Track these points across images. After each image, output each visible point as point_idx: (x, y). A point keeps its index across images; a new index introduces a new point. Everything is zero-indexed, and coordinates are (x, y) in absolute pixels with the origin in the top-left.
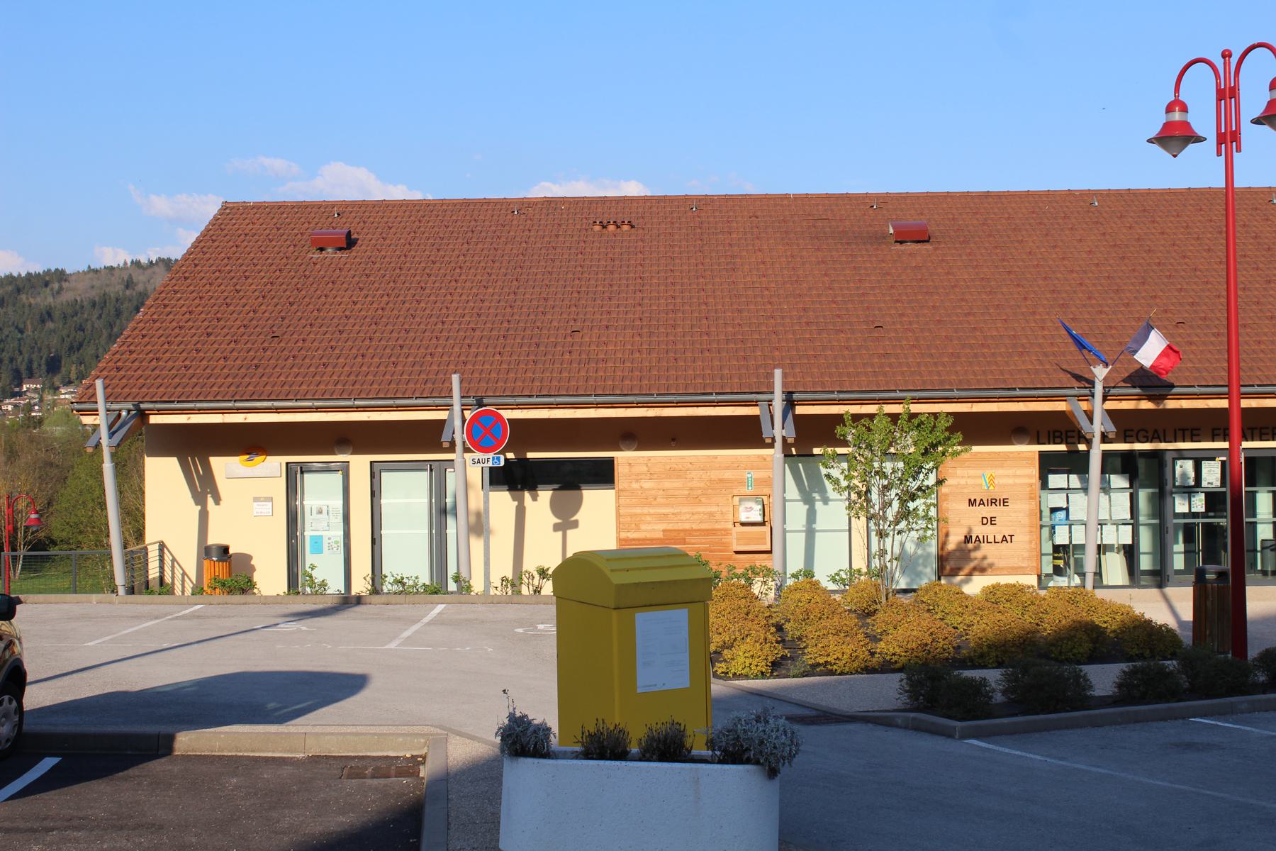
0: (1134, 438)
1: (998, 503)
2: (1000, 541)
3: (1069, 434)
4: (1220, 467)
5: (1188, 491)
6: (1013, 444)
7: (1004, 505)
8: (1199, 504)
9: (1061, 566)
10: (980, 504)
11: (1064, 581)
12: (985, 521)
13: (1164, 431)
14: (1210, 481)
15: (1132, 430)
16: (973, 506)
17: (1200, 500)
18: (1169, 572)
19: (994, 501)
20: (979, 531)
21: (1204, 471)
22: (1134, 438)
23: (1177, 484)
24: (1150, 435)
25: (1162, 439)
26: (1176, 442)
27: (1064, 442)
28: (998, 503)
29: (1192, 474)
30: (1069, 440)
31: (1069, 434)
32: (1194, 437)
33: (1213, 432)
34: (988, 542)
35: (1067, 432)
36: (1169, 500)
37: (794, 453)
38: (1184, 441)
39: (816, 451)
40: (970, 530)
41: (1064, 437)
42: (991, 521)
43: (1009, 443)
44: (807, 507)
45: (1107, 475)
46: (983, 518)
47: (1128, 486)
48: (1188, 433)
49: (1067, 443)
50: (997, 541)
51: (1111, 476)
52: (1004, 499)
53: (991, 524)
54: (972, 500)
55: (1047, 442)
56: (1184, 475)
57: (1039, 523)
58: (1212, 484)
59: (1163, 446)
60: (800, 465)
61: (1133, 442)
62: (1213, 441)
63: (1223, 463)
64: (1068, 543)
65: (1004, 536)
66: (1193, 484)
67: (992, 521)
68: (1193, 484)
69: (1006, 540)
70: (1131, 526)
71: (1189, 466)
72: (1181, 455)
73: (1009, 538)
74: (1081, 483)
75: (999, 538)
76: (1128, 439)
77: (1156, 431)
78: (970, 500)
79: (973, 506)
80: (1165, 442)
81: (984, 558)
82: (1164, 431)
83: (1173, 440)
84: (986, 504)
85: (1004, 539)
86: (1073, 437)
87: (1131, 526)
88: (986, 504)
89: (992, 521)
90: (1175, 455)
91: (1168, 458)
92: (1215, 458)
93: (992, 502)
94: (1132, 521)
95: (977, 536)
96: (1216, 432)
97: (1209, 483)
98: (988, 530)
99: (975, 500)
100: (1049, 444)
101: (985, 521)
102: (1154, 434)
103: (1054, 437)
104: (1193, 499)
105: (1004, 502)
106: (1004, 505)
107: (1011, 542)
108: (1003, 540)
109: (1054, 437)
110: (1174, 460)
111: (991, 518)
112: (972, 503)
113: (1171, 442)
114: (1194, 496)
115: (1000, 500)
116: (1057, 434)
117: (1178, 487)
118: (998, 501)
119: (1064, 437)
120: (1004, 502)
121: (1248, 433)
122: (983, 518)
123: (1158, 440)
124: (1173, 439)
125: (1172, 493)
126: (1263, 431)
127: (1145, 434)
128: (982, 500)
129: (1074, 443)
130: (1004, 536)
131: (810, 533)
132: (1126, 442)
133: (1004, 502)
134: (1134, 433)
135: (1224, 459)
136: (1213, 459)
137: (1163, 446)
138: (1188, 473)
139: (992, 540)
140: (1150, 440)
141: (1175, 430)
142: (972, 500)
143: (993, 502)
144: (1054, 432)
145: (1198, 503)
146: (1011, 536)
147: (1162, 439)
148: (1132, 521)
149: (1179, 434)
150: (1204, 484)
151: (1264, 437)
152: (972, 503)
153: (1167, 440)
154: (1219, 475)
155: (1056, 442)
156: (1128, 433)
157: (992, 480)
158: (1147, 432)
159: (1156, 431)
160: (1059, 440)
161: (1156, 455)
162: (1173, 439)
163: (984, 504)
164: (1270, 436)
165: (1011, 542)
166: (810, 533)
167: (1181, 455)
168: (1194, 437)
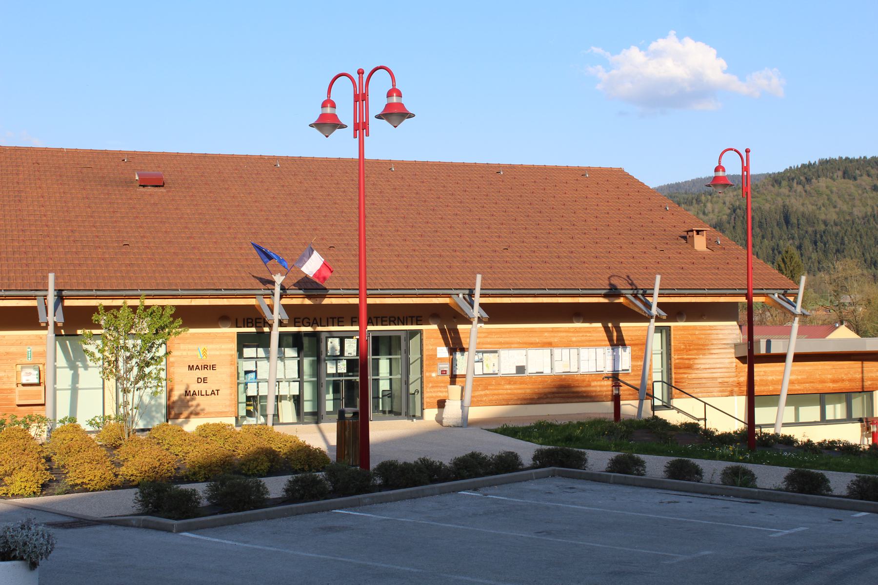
0: (301, 324)
1: (208, 368)
5: (336, 359)
6: (220, 328)
8: (342, 367)
9: (252, 410)
10: (196, 369)
13: (321, 319)
15: (300, 318)
16: (191, 370)
17: (343, 365)
18: (323, 413)
20: (194, 387)
22: (301, 324)
23: (329, 354)
24: (311, 322)
25: (319, 325)
26: (328, 326)
27: (254, 325)
28: (208, 368)
29: (338, 348)
30: (258, 325)
31: (258, 321)
32: (340, 323)
34: (201, 395)
36: (323, 365)
37: (63, 333)
38: (333, 326)
39: (79, 332)
40: (188, 386)
41: (254, 322)
42: (204, 380)
43: (218, 327)
44: (72, 372)
45: (283, 348)
46: (198, 378)
47: (297, 356)
49: (256, 327)
51: (286, 349)
54: (191, 366)
55: (242, 326)
56: (333, 348)
58: (351, 354)
59: (319, 329)
60: (68, 342)
61: (300, 326)
63: (358, 339)
64: (256, 395)
66: (339, 354)
67: (205, 380)
68: (339, 354)
69: (214, 394)
70: (298, 383)
72: (331, 335)
73: (216, 392)
75: (209, 392)
77: (315, 319)
78: (189, 366)
79: (191, 370)
81: (198, 405)
82: (321, 319)
84: (200, 368)
85: (213, 393)
87: (298, 383)
88: (200, 369)
89: (205, 380)
90: (327, 335)
91: (323, 336)
92: (353, 337)
93: (204, 368)
94: (299, 379)
95: (194, 391)
97: (349, 353)
98: (202, 387)
99: (193, 366)
100: (244, 327)
102: (314, 321)
103: (248, 323)
104: (338, 364)
105: (213, 367)
107: (218, 394)
108: (212, 394)
110: (327, 338)
111: (204, 378)
112: (191, 368)
113: (325, 326)
114: (339, 362)
117: (329, 356)
118: (209, 367)
119: (254, 322)
120: (213, 367)
121: (374, 321)
122: (198, 378)
125: (325, 360)
126: (384, 319)
127: (308, 320)
128: (197, 366)
129: (261, 327)
130: (213, 391)
131: (74, 391)
132: (295, 326)
133: (213, 367)
134: (301, 320)
135: (358, 337)
136: (352, 337)
137: (319, 329)
138: (336, 347)
142: (191, 366)
143: (205, 367)
144: (247, 319)
146: (218, 390)
147: (319, 325)
148: (299, 379)
149: (330, 320)
150: (346, 354)
152: (191, 368)
153: (322, 325)
156: (297, 320)
158: (309, 320)
159: (315, 319)
160: (250, 325)
161: (315, 335)
163: (199, 369)
165: (218, 394)
166: (74, 391)
167: (331, 335)
168: (340, 323)
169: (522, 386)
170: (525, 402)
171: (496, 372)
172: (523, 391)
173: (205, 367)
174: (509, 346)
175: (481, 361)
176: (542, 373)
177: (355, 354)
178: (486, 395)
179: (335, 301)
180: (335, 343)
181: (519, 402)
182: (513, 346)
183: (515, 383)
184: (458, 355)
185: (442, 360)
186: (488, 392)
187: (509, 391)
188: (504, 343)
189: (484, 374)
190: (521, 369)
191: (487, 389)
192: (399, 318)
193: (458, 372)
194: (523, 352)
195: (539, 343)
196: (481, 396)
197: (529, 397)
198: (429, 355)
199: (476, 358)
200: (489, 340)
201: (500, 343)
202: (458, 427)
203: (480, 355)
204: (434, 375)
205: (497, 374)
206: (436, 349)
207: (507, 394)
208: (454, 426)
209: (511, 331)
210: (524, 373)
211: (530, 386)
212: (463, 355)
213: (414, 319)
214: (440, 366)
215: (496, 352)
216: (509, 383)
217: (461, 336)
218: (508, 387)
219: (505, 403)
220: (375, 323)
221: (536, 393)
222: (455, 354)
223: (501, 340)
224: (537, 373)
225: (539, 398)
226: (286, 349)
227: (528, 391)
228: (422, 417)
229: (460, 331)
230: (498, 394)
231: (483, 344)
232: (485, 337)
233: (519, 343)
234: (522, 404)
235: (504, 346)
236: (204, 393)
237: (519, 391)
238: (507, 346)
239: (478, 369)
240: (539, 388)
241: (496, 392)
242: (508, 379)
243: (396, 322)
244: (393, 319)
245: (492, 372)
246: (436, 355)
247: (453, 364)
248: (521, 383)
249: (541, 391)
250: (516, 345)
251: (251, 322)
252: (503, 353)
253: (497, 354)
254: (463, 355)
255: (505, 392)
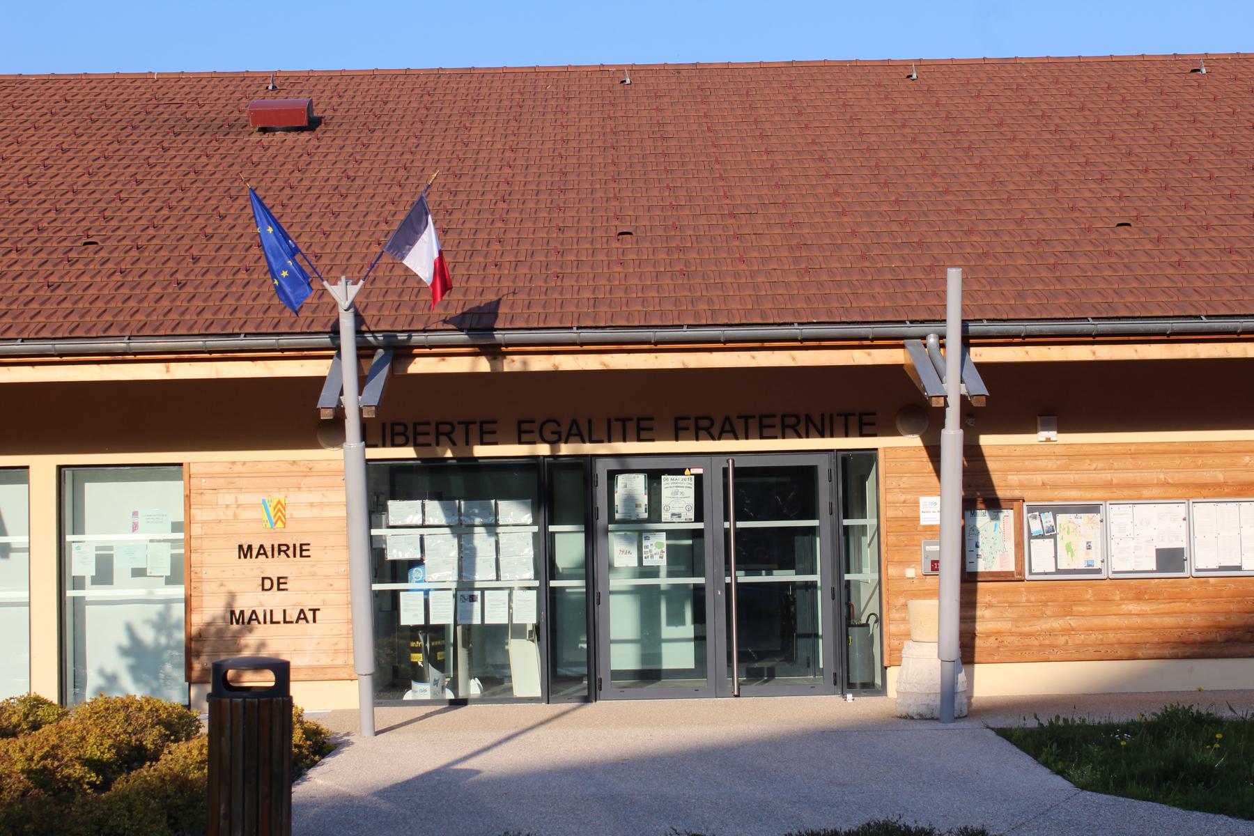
0: (536, 436)
1: (290, 552)
2: (295, 619)
3: (420, 428)
4: (693, 486)
5: (637, 528)
6: (320, 447)
7: (301, 556)
8: (656, 550)
9: (420, 664)
10: (259, 554)
11: (426, 691)
12: (267, 584)
13: (590, 422)
14: (676, 511)
15: (533, 421)
16: (245, 556)
17: (659, 545)
18: (603, 674)
19: (284, 548)
21: (666, 493)
22: (536, 436)
23: (617, 516)
24: (564, 430)
25: (586, 438)
26: (610, 441)
27: (411, 441)
28: (290, 552)
29: (643, 500)
30: (421, 439)
31: (420, 428)
32: (642, 432)
33: (676, 424)
34: (272, 622)
35: (416, 425)
38: (625, 440)
40: (232, 596)
41: (410, 433)
42: (279, 583)
43: (316, 446)
45: (457, 501)
46: (263, 579)
47: (530, 521)
48: (631, 426)
49: (416, 445)
50: (287, 620)
51: (500, 503)
52: (301, 545)
53: (279, 589)
54: (245, 548)
55: (380, 443)
56: (630, 500)
57: (516, 585)
58: (679, 516)
59: (588, 448)
61: (533, 443)
62: (677, 439)
63: (699, 479)
64: (506, 621)
65: (302, 611)
66: (645, 516)
67: (280, 583)
68: (645, 516)
69: (305, 618)
70: (535, 592)
71: (638, 483)
72: (624, 465)
73: (310, 615)
74: (447, 516)
75: (293, 615)
76: (525, 437)
78: (241, 547)
79: (245, 556)
80: (591, 441)
81: (262, 645)
82: (590, 422)
83: (606, 438)
84: (269, 554)
85: (302, 616)
86: (427, 434)
87: (535, 592)
88: (269, 554)
89: (280, 583)
90: (613, 465)
91: (601, 469)
92: (685, 470)
93: (280, 551)
94: (536, 583)
95: (254, 612)
96: (682, 423)
97: (673, 515)
98: (274, 601)
99: (250, 547)
100: (384, 445)
101: (267, 584)
102: (571, 429)
103: (393, 435)
104: (645, 543)
105: (302, 550)
106: (301, 556)
107: (314, 621)
108: (299, 618)
109: (393, 435)
110: (612, 475)
111: (279, 578)
112: (245, 551)
113: (601, 441)
114: (648, 538)
115: (294, 545)
116: (399, 429)
118: (292, 549)
119: (410, 433)
120: (302, 550)
122: (263, 579)
123: (578, 438)
124: (604, 436)
125: (607, 531)
126: (766, 421)
128: (262, 546)
129: (429, 445)
130: (302, 611)
132: (520, 443)
133: (302, 550)
134: (536, 426)
135: (700, 471)
136: (680, 472)
137: (588, 448)
138: (637, 497)
139: (281, 619)
140: (564, 437)
141: (609, 421)
142: (245, 548)
143: (282, 549)
144: (393, 425)
145: (655, 550)
146: (314, 611)
147: (586, 438)
148: (536, 583)
149: (617, 427)
150: (665, 516)
151: (766, 432)
152: (245, 551)
153: (594, 438)
154: (691, 501)
155: (396, 442)
156: (525, 426)
157: (279, 510)
158: (559, 425)
160: (399, 439)
161: (584, 464)
162: (604, 436)
163: (265, 553)
164: (778, 430)
165: (314, 621)
167: (624, 465)
168: (642, 432)
169: (1176, 606)
170: (1188, 651)
171: (1097, 565)
172: (1179, 621)
173: (282, 549)
174: (1134, 493)
175: (1050, 534)
176: (1239, 568)
177: (691, 515)
178: (1069, 631)
179: (539, 364)
180: (633, 486)
181: (1167, 652)
182: (1146, 493)
183: (1155, 597)
184: (983, 519)
185: (934, 532)
186: (1073, 622)
187: (1139, 620)
188: (1119, 486)
189: (1059, 571)
190: (1170, 559)
191: (1071, 614)
192: (809, 419)
193: (982, 567)
194: (1180, 510)
195: (1225, 484)
196: (1051, 633)
197: (1198, 638)
198: (896, 519)
199: (1036, 527)
200: (1072, 477)
201: (1108, 486)
202: (932, 719)
203: (1048, 518)
204: (910, 572)
205: (1099, 571)
206: (917, 502)
207: (1129, 628)
208: (922, 718)
209: (1110, 454)
210: (1182, 570)
211: (1204, 608)
212: (995, 518)
213: (854, 420)
214: (929, 548)
215: (1093, 509)
216: (1138, 598)
217: (991, 465)
218: (1133, 607)
219: (1126, 653)
220: (740, 431)
221: (1219, 628)
222: (974, 515)
223: (1108, 476)
224: (1222, 568)
225: (1228, 641)
226: (504, 505)
227: (1196, 621)
228: (882, 690)
229: (986, 452)
230: (1105, 629)
231: (1055, 487)
232: (1059, 469)
233: (1166, 484)
234: (1176, 657)
235: (1118, 493)
236: (278, 616)
237: (1169, 621)
238: (1127, 493)
239: (1042, 558)
240: (1228, 613)
241: (1098, 622)
242: (1133, 586)
243: (801, 429)
244: (792, 421)
245: (1082, 566)
246: (918, 519)
247: (968, 542)
248: (1173, 598)
249: (1235, 620)
250: (1155, 492)
251: (404, 434)
252: (1118, 514)
253: (1097, 517)
254: (995, 518)
255: (1125, 622)
